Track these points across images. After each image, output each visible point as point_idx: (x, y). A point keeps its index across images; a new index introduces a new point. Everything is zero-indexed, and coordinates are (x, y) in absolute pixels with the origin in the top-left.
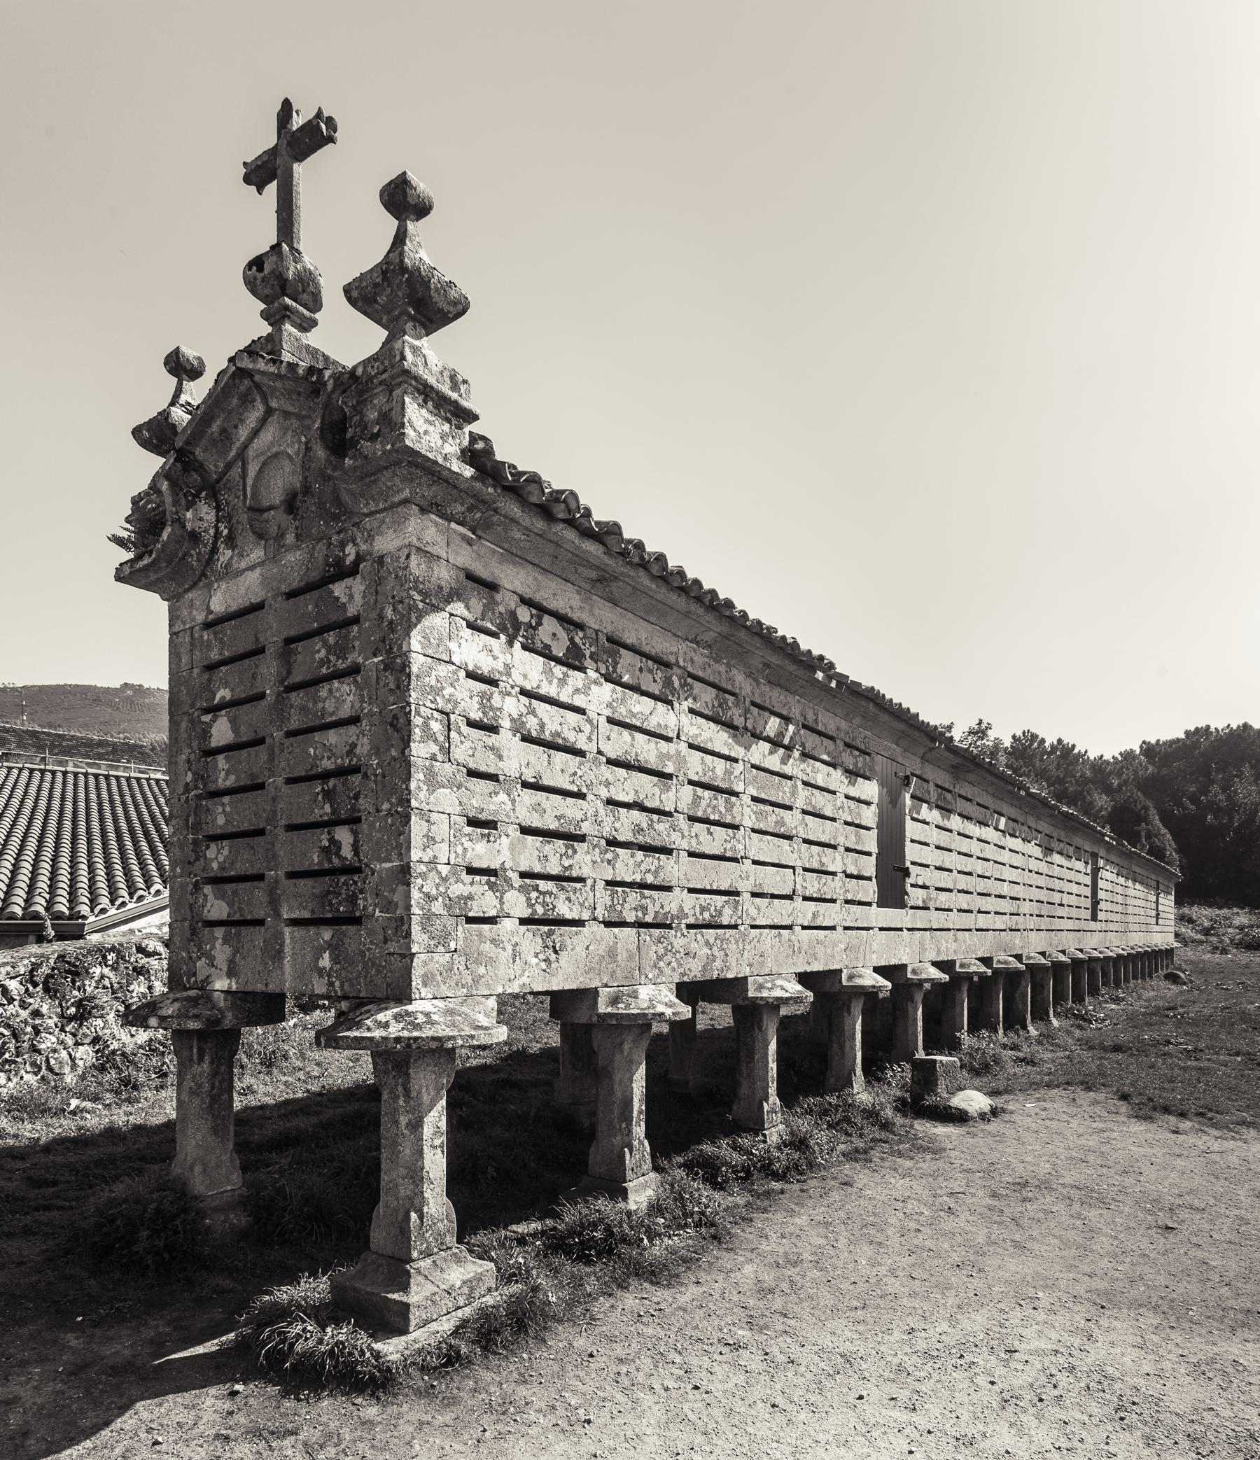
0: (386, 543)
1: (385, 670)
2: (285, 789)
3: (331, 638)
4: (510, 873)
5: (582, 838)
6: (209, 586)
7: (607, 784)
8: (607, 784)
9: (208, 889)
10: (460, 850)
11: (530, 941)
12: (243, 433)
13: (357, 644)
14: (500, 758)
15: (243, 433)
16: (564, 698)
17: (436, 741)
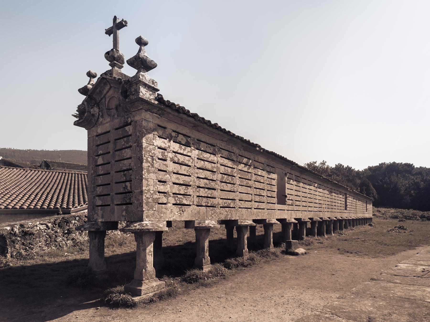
0: (137, 118)
2: (115, 174)
3: (125, 139)
4: (170, 193)
5: (190, 186)
6: (97, 127)
7: (197, 173)
8: (197, 173)
9: (97, 198)
10: (156, 187)
11: (176, 209)
12: (105, 92)
14: (167, 167)
15: (105, 92)
16: (185, 153)
17: (150, 163)
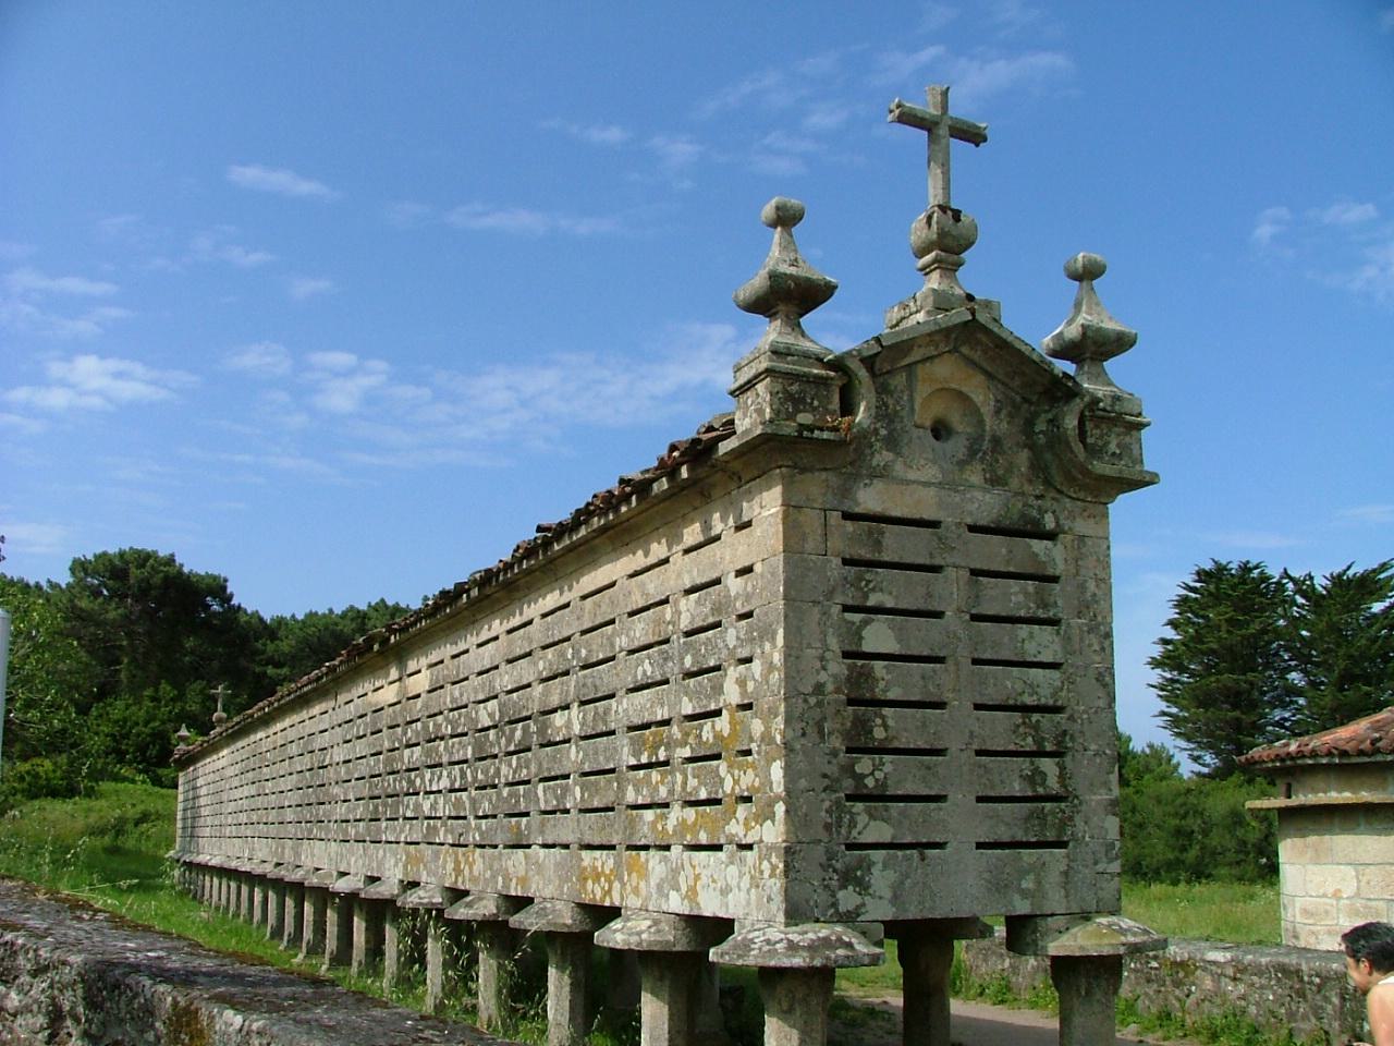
1: (1089, 633)
9: (859, 806)
13: (1060, 603)
